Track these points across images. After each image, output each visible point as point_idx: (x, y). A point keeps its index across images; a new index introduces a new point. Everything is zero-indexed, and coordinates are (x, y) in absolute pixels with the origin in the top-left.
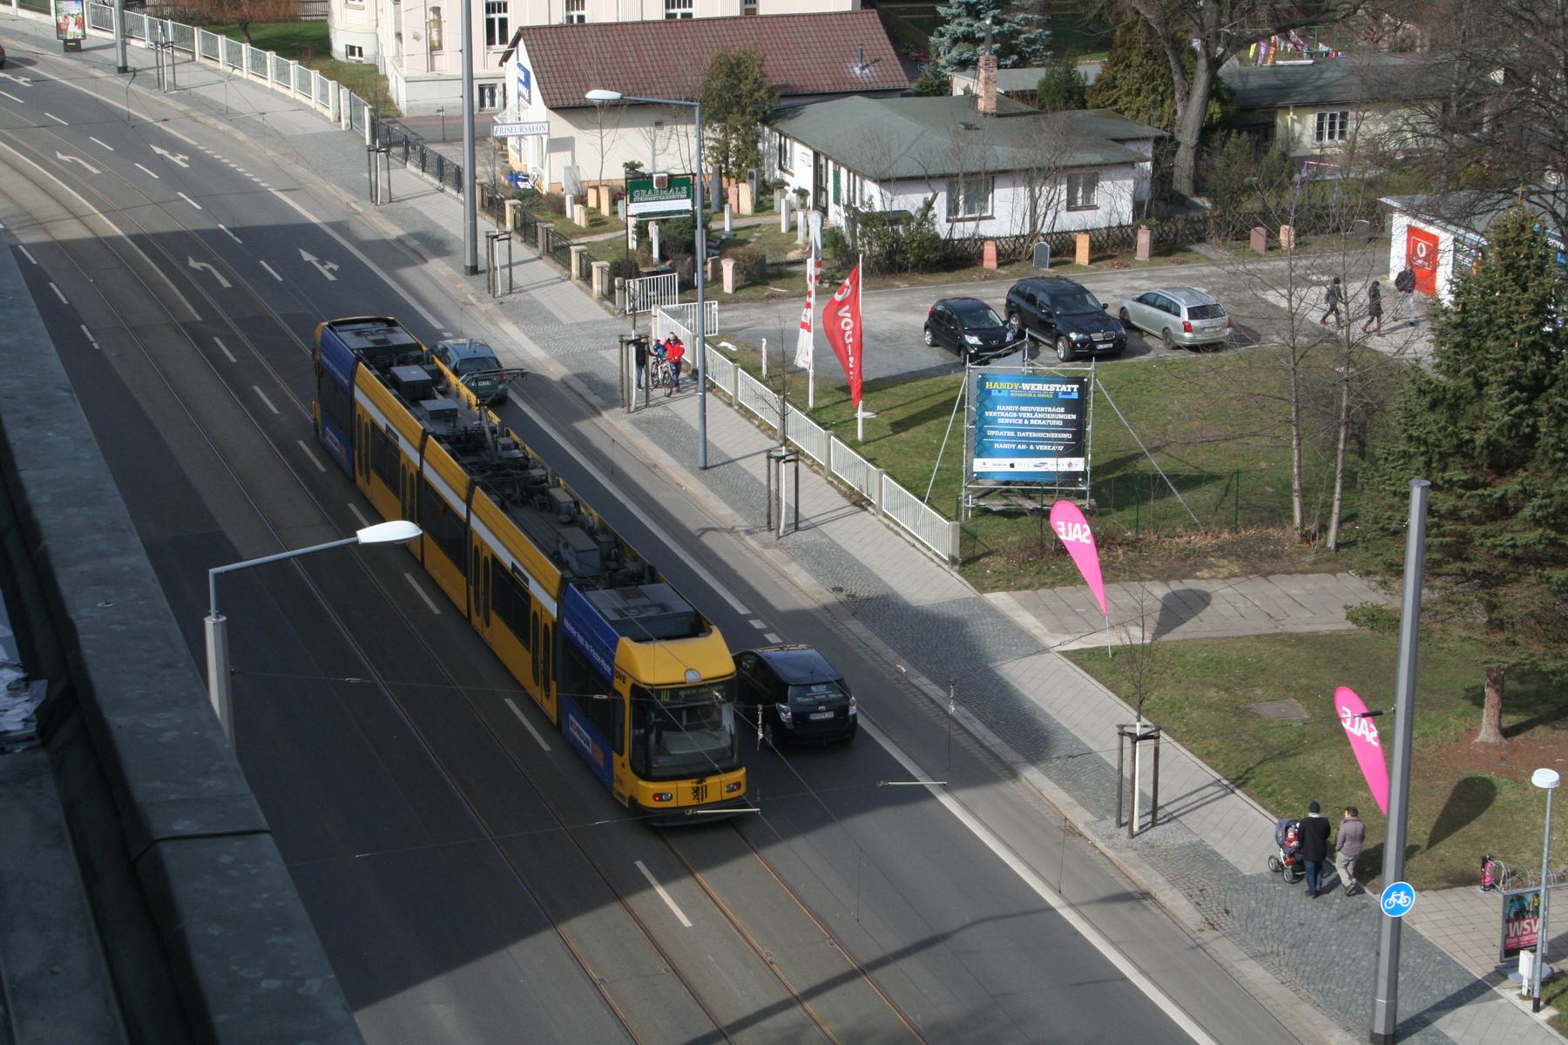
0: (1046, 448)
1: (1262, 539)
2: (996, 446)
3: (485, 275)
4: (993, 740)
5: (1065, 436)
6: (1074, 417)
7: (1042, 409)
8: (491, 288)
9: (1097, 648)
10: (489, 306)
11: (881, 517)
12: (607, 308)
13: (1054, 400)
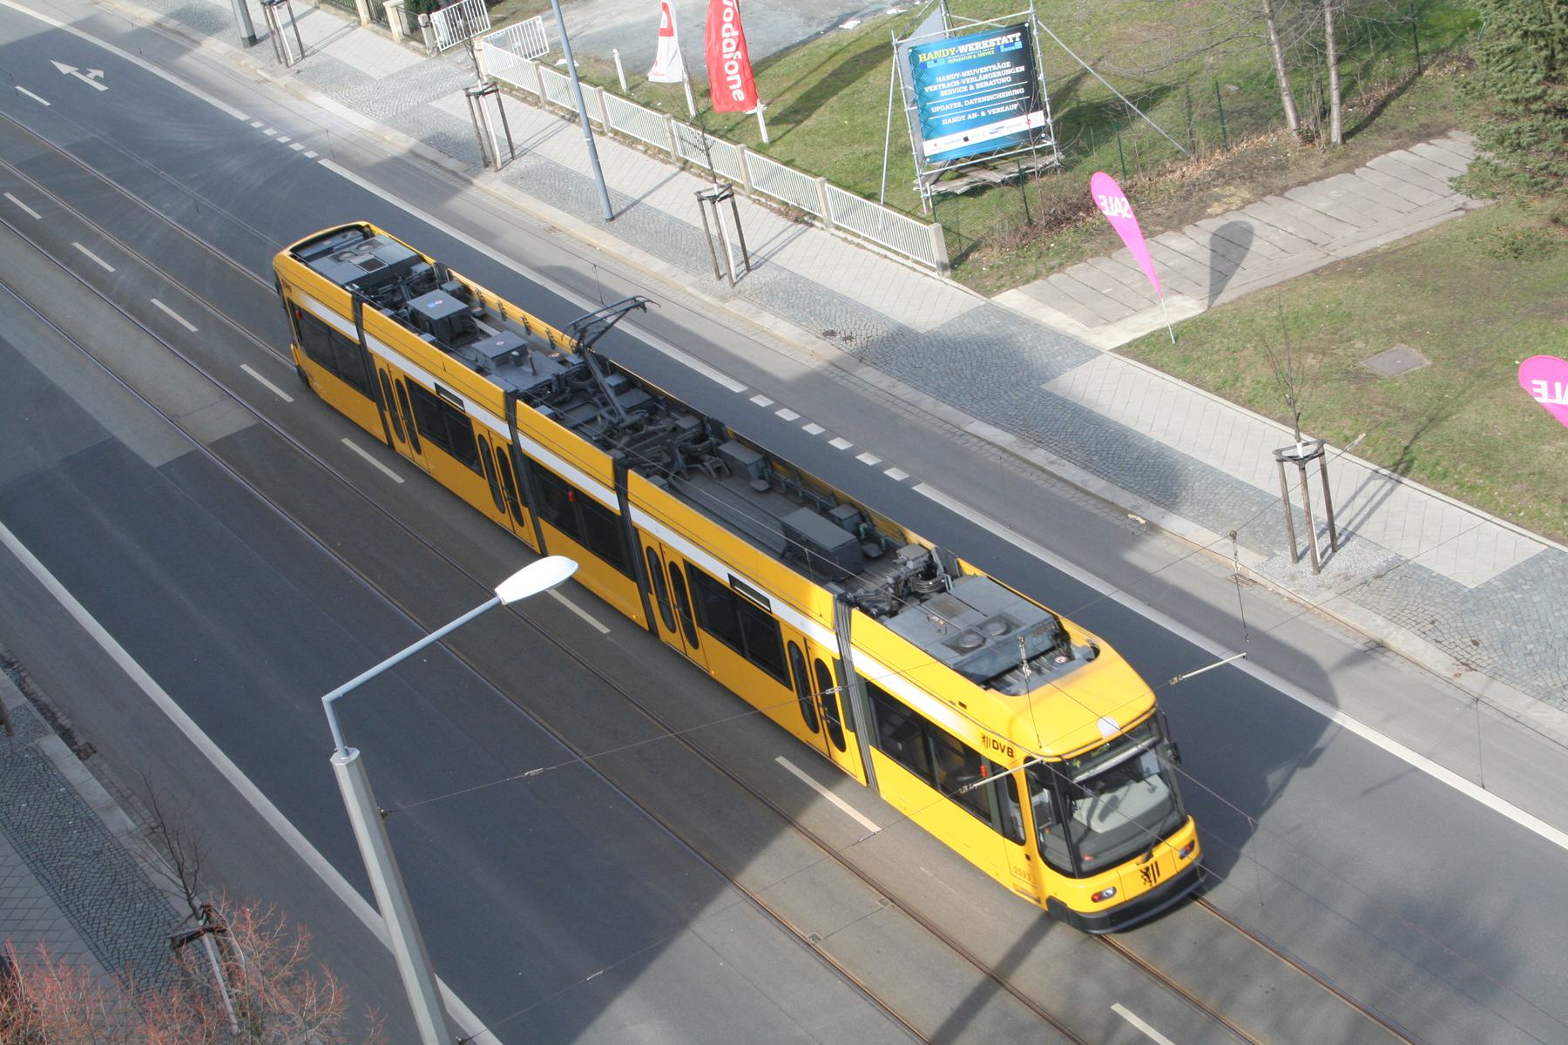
0: (1002, 110)
1: (1258, 152)
2: (944, 122)
3: (269, 42)
4: (1096, 484)
5: (1017, 92)
6: (1022, 69)
7: (986, 69)
8: (281, 56)
9: (1151, 335)
10: (286, 79)
11: (833, 231)
12: (415, 49)
13: (998, 56)
